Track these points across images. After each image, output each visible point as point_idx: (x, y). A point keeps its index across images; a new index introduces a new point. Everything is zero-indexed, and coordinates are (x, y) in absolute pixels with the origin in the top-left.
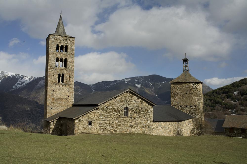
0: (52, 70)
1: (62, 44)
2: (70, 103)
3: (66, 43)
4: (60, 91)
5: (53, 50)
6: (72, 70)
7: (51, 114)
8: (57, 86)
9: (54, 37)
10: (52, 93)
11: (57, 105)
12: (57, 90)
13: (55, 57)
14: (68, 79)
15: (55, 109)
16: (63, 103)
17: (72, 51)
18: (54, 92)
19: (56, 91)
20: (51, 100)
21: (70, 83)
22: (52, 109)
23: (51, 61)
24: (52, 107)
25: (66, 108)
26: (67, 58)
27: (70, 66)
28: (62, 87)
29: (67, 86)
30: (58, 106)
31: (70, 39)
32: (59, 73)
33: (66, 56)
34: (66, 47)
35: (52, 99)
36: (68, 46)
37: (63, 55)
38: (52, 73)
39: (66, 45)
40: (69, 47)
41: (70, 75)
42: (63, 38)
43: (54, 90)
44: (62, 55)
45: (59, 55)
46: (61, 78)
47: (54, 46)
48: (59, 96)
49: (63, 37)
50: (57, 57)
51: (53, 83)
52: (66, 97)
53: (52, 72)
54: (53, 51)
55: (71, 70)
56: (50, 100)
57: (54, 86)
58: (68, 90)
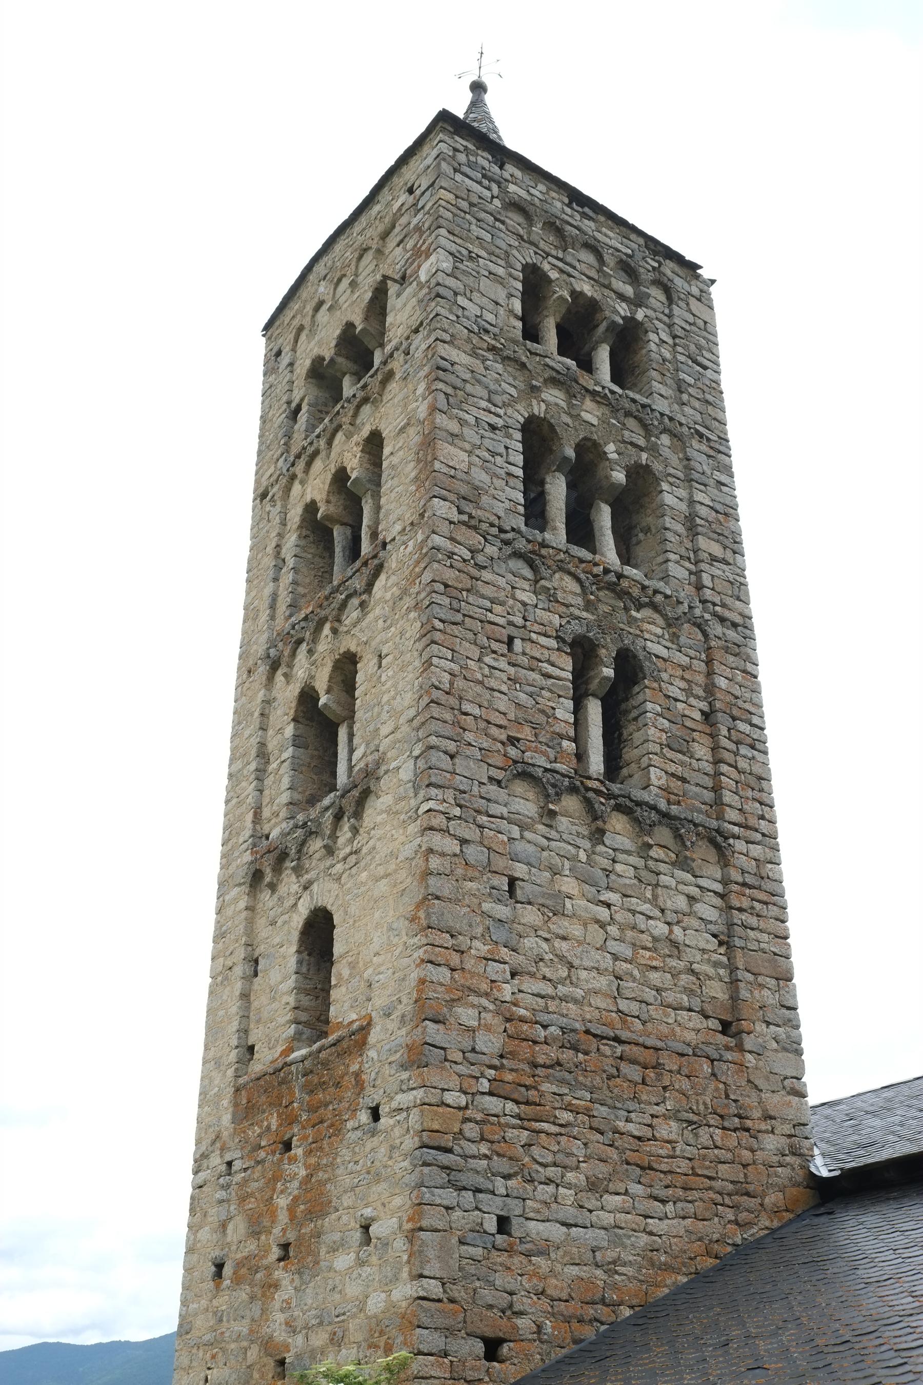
0: (491, 550)
1: (587, 289)
2: (771, 1143)
3: (622, 297)
4: (603, 913)
5: (491, 306)
6: (731, 634)
7: (492, 1348)
8: (563, 822)
9: (496, 169)
10: (502, 911)
11: (577, 1148)
12: (569, 885)
13: (514, 400)
14: (702, 751)
15: (556, 1232)
16: (669, 1129)
17: (697, 404)
18: (530, 916)
19: (554, 907)
20: (490, 1043)
21: (732, 815)
22: (503, 1224)
23: (462, 422)
24: (500, 1185)
25: (713, 1228)
26: (657, 467)
27: (706, 580)
28: (640, 863)
29: (702, 852)
30: (602, 1170)
31: (669, 273)
32: (576, 628)
33: (642, 442)
34: (627, 340)
35: (496, 1022)
36: (652, 336)
37: (606, 410)
38: (488, 591)
39: (623, 309)
40: (668, 355)
41: (710, 689)
42: (592, 224)
43: (520, 870)
44: (591, 413)
45: (554, 396)
46: (594, 710)
47: (501, 271)
48: (590, 993)
49: (586, 210)
50: (539, 409)
51: (513, 752)
52: (691, 1028)
53: (487, 575)
54: (490, 317)
55: (717, 629)
56: (472, 1030)
57: (525, 803)
58: (708, 910)
